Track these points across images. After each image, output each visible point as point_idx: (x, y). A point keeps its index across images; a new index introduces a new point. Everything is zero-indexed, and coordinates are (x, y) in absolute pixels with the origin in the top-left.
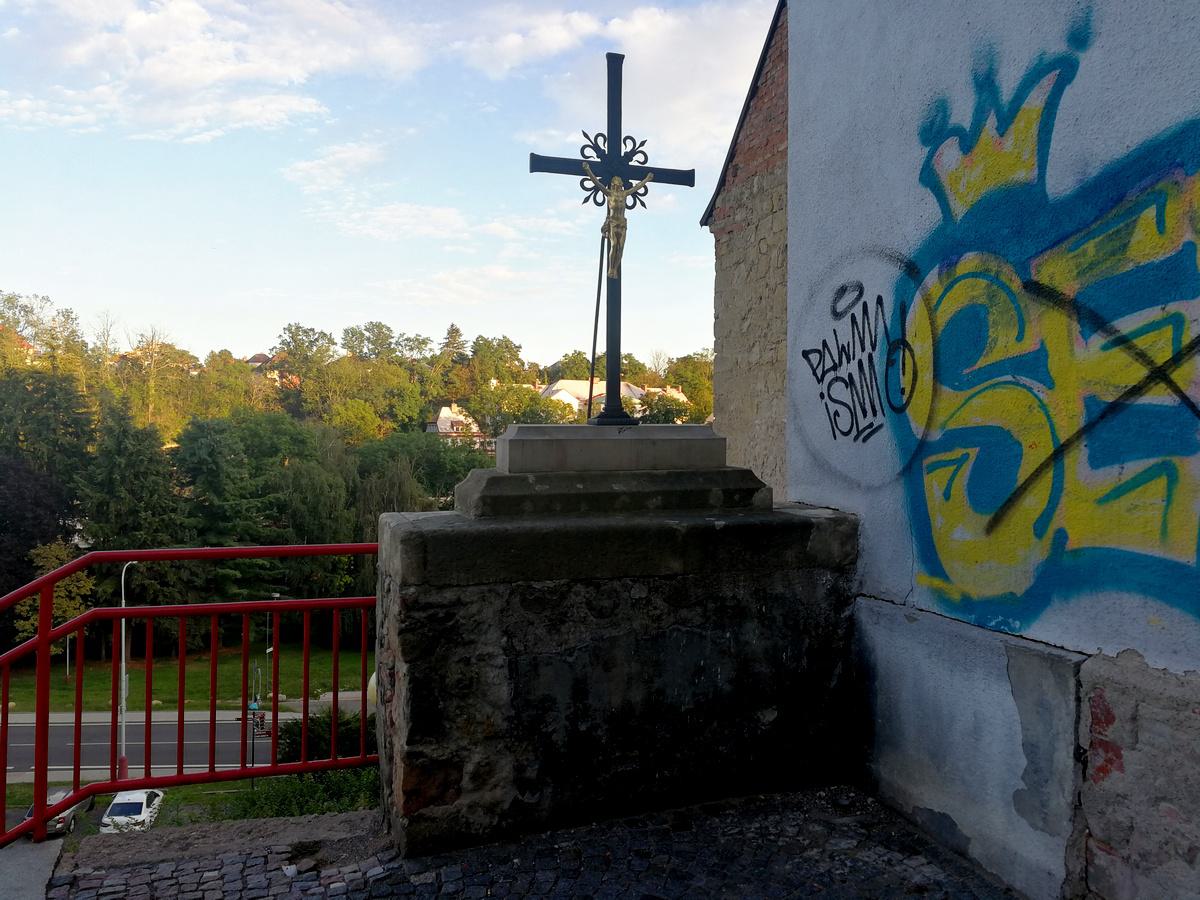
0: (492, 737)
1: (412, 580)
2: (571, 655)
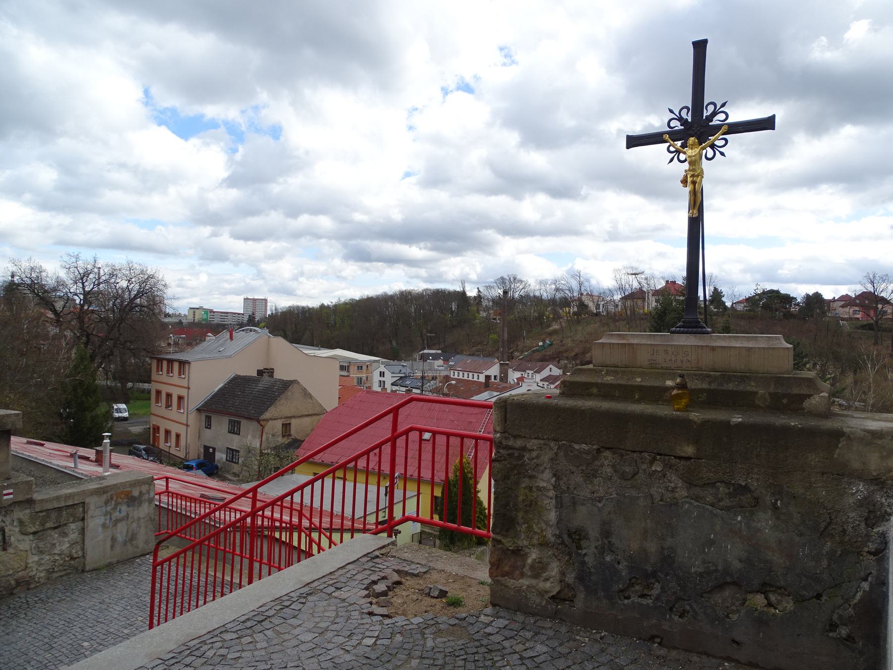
1: (498, 429)
2: (600, 502)
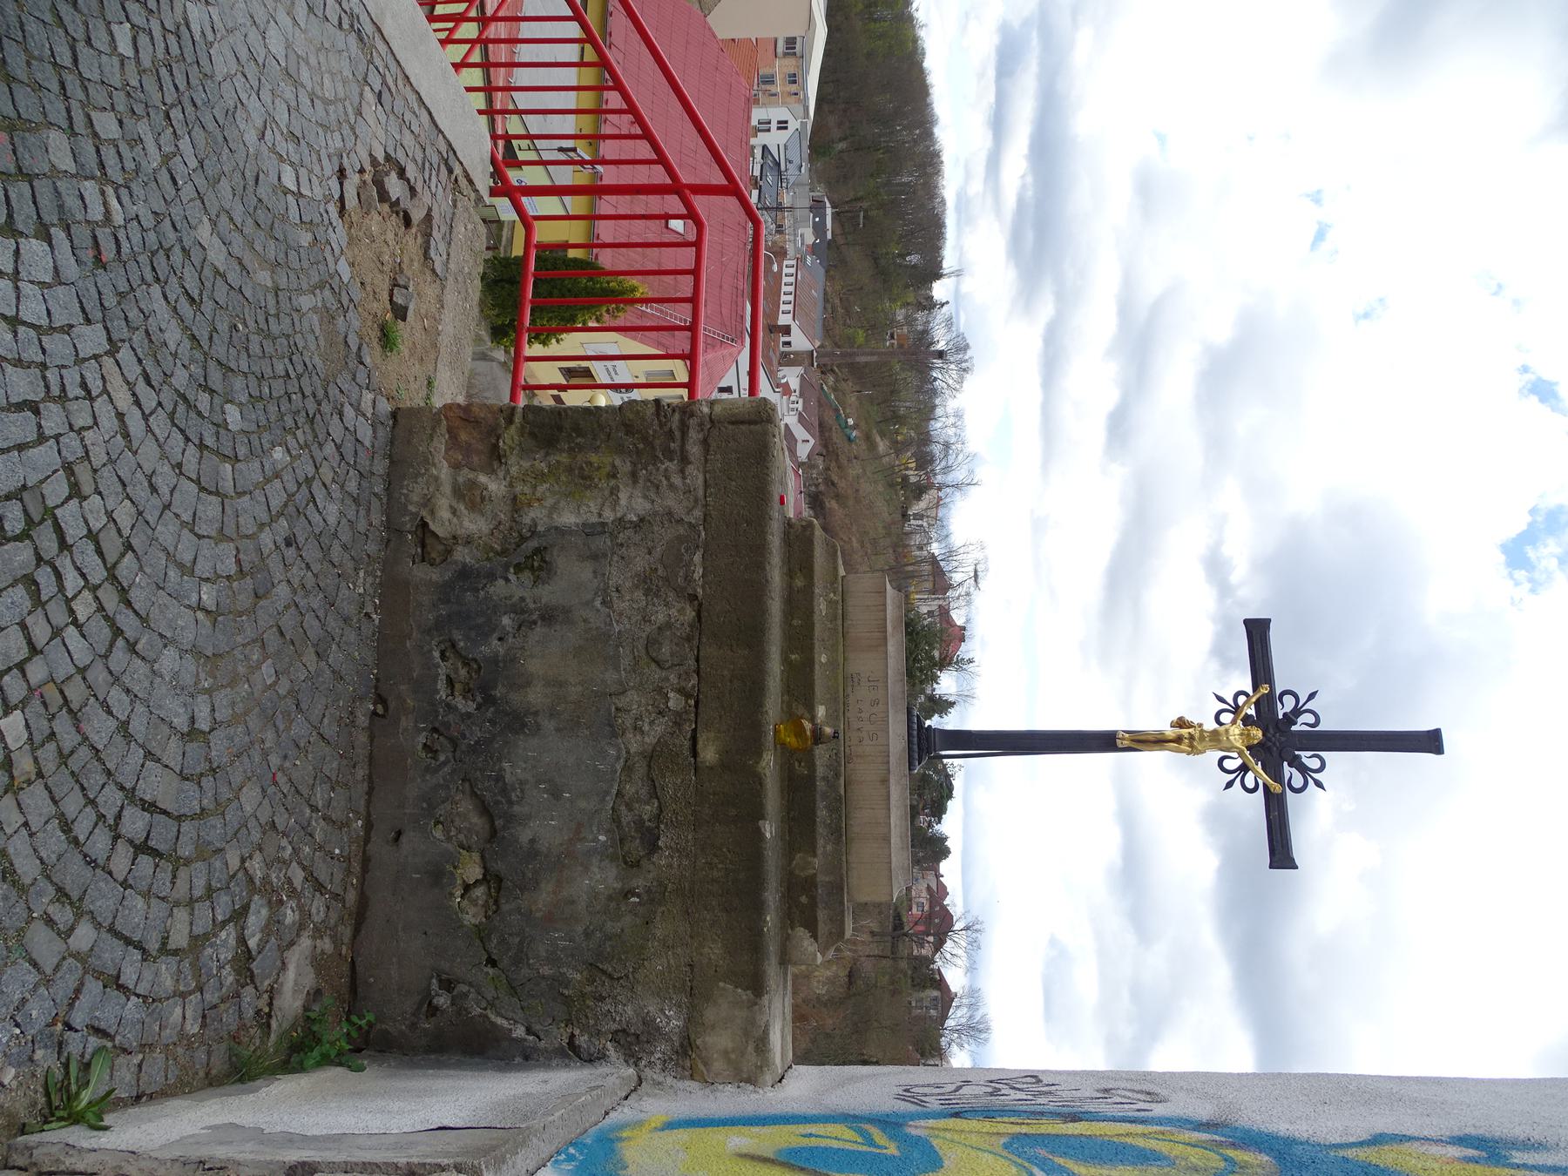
0: (516, 504)
1: (718, 409)
2: (604, 603)
